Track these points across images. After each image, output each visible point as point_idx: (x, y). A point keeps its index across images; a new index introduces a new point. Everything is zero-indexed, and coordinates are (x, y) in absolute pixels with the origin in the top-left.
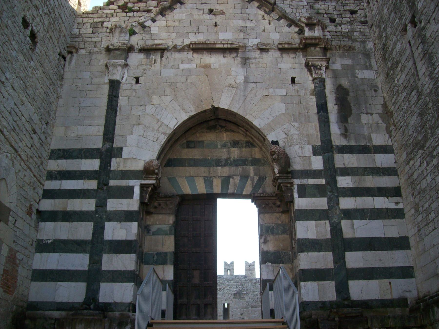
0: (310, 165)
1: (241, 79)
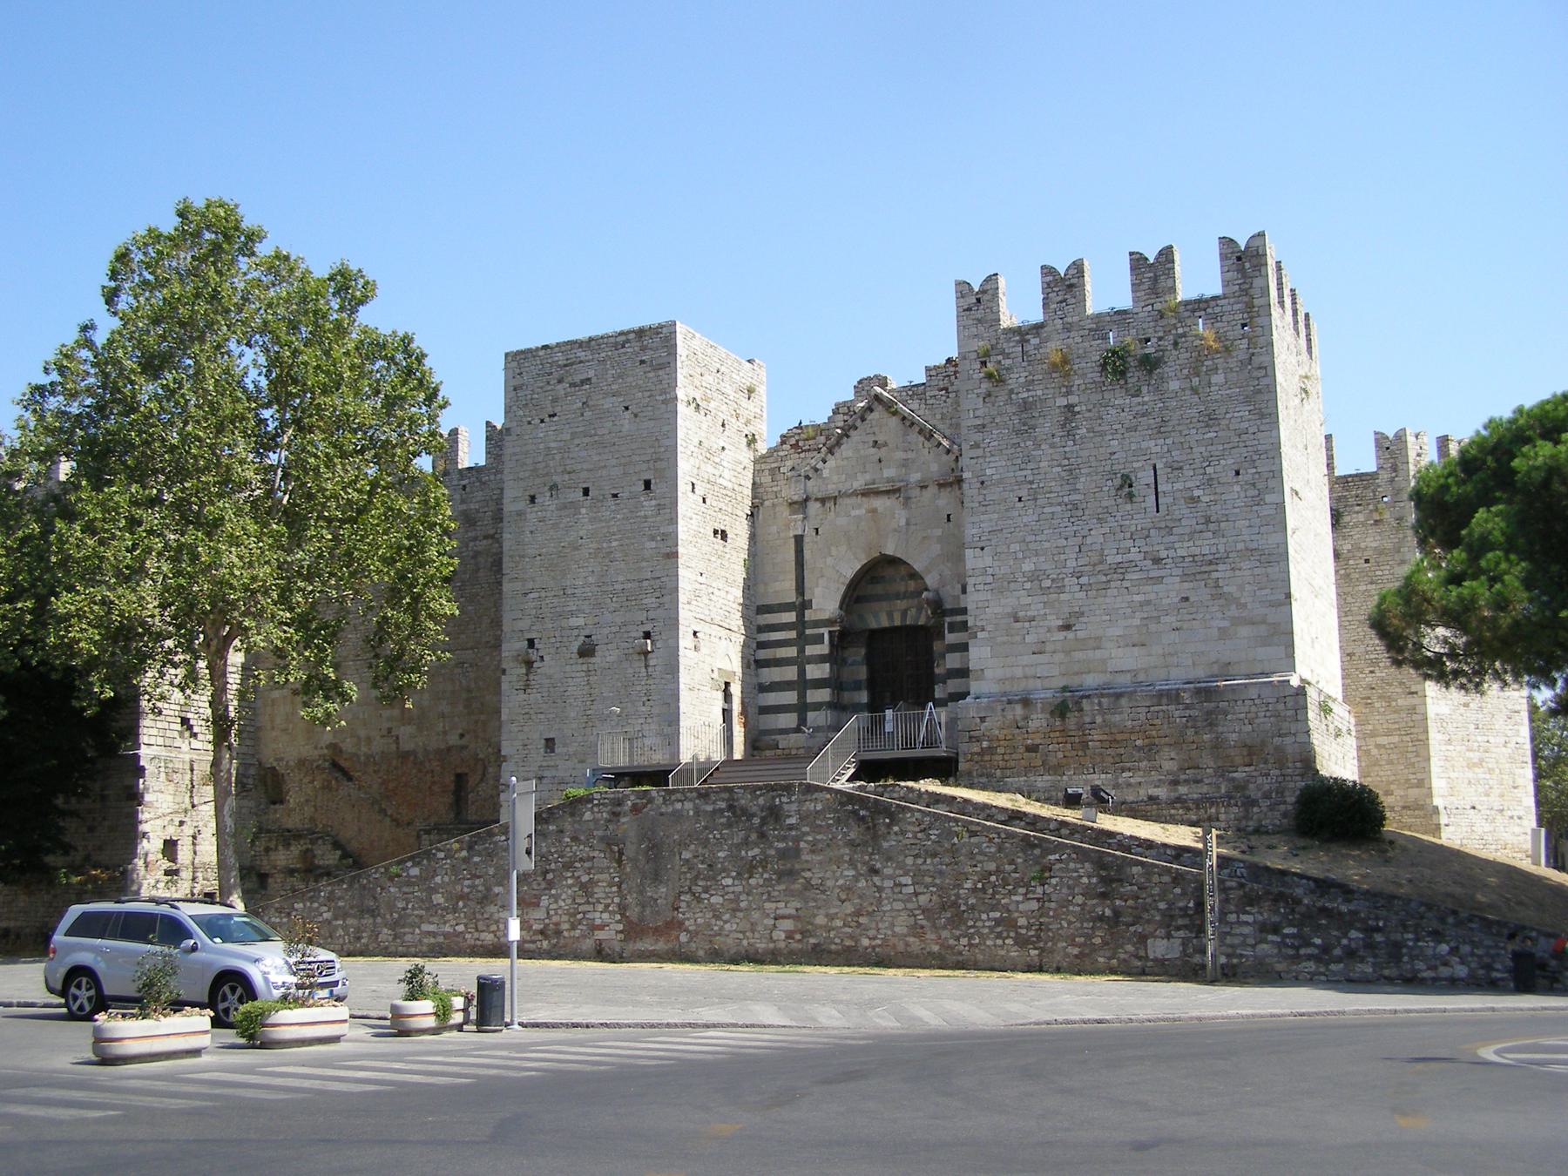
0: (959, 603)
1: (903, 522)
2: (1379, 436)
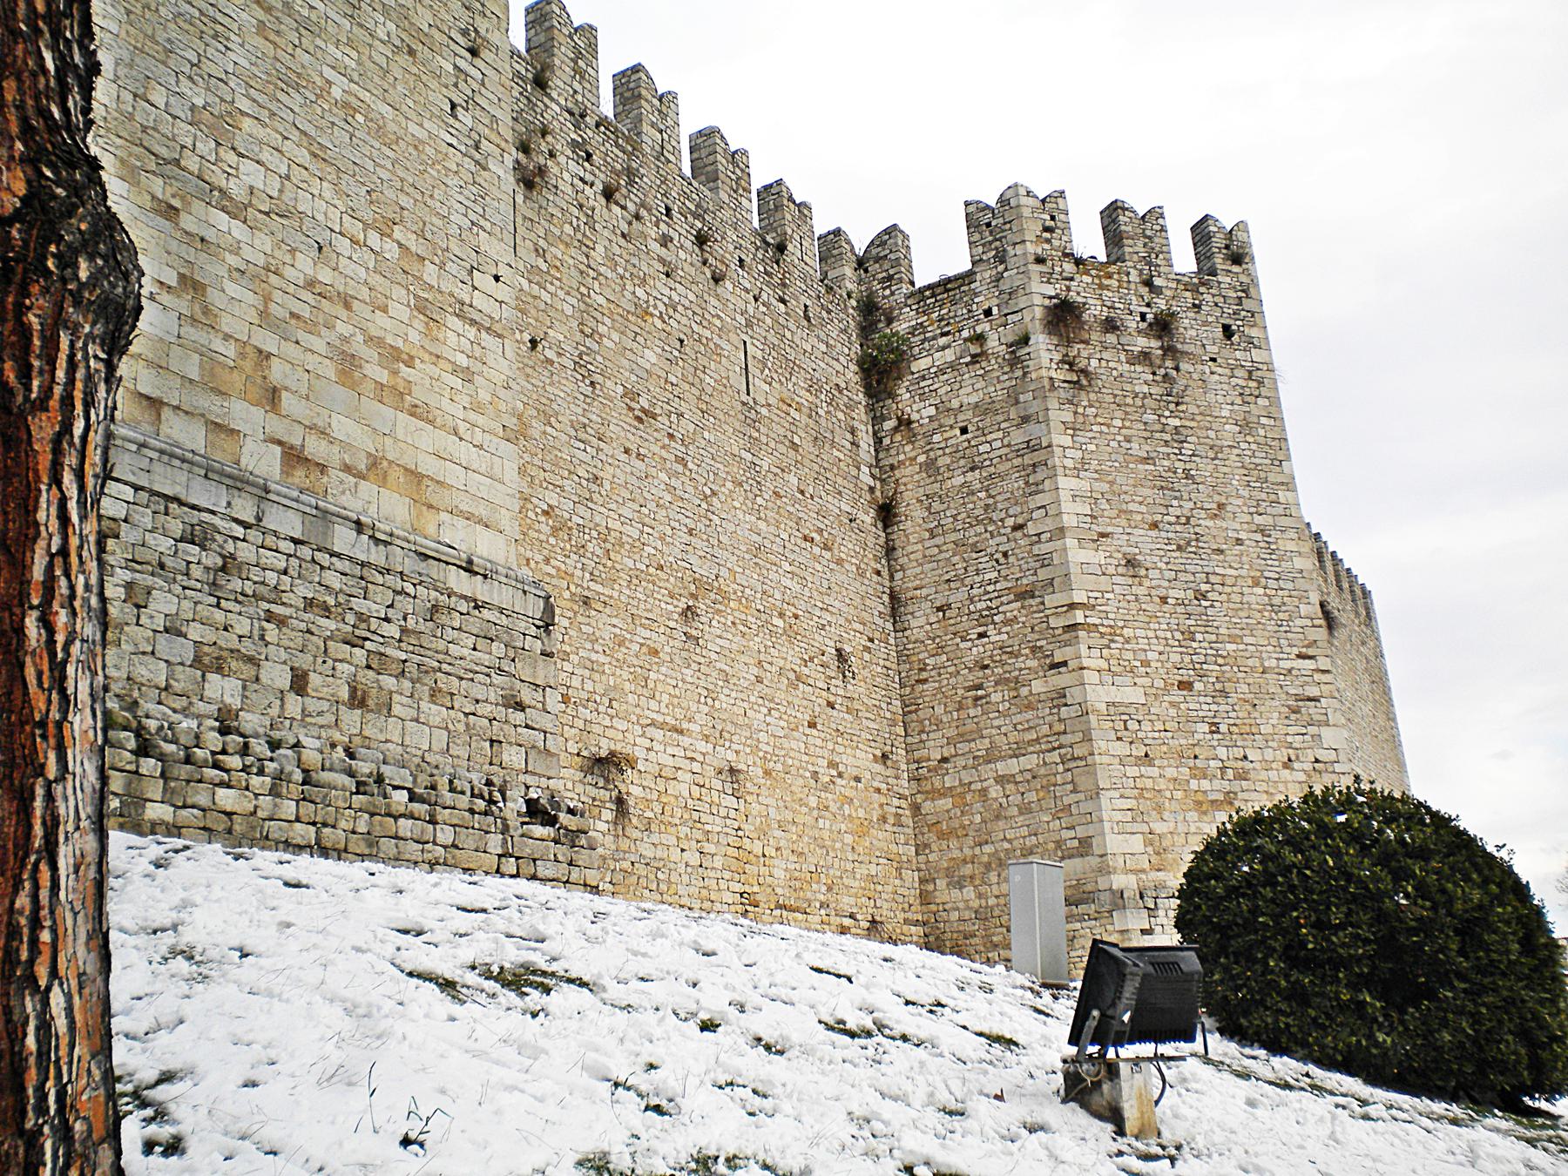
2: (971, 209)
